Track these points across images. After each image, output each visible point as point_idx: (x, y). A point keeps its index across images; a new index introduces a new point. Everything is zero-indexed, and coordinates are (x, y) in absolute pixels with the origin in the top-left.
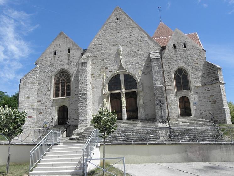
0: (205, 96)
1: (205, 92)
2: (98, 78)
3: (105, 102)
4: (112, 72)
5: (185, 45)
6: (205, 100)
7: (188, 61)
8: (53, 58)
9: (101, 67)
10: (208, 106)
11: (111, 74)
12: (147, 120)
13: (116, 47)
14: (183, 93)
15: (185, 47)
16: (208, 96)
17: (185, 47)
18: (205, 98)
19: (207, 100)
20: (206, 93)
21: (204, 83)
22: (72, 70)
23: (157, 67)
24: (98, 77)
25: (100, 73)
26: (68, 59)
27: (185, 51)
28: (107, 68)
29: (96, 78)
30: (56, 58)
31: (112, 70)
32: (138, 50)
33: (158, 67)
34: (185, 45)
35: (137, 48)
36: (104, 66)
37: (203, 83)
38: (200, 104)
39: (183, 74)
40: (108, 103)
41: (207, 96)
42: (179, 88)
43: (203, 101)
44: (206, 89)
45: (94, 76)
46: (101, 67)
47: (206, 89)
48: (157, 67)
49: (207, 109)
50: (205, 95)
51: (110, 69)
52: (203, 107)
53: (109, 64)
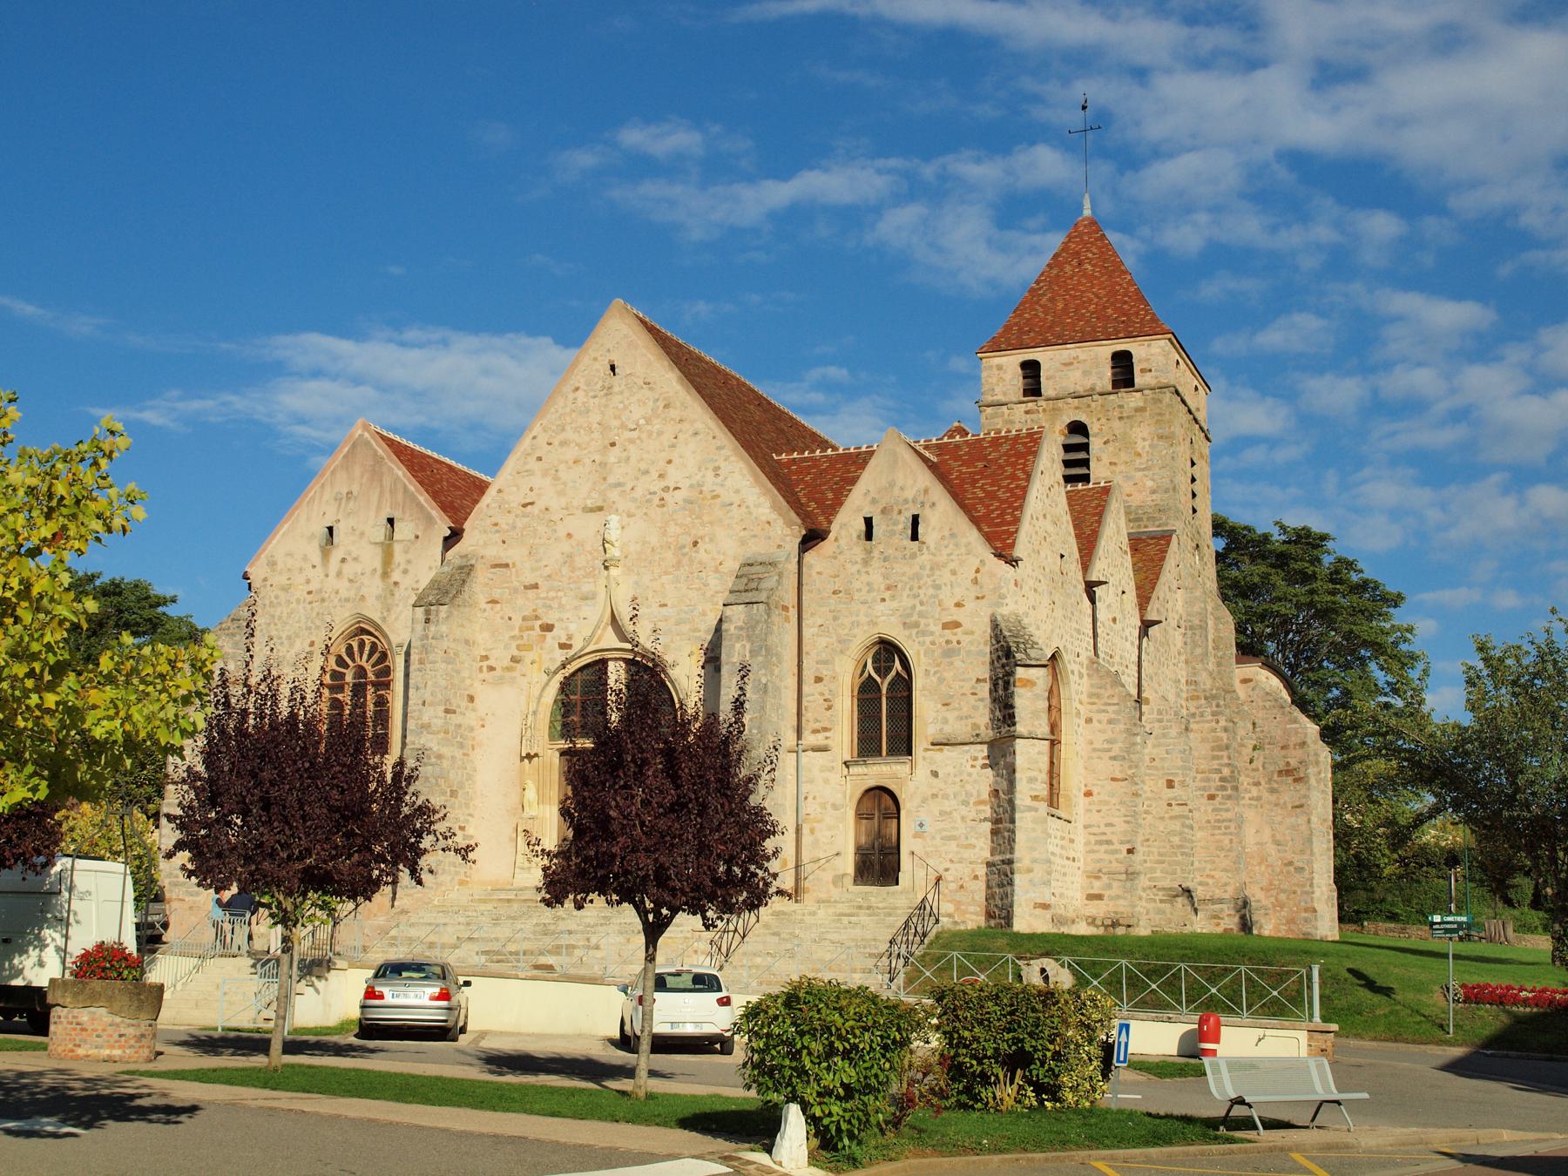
0: (968, 794)
1: (970, 775)
2: (508, 675)
3: (531, 794)
4: (569, 647)
5: (915, 520)
6: (964, 810)
7: (919, 607)
8: (316, 557)
9: (524, 619)
10: (973, 841)
11: (560, 656)
12: (882, 864)
13: (595, 520)
14: (882, 771)
15: (915, 537)
16: (979, 795)
17: (915, 537)
18: (965, 803)
19: (973, 815)
20: (975, 776)
21: (975, 726)
22: (400, 628)
23: (744, 646)
24: (508, 669)
25: (516, 653)
26: (385, 575)
27: (913, 556)
28: (548, 628)
29: (498, 673)
30: (337, 555)
31: (570, 637)
32: (695, 544)
33: (748, 646)
34: (915, 520)
35: (693, 532)
36: (537, 618)
37: (969, 728)
38: (944, 830)
39: (893, 673)
40: (541, 799)
41: (975, 793)
42: (868, 746)
43: (955, 814)
44: (975, 759)
45: (491, 662)
46: (524, 619)
47: (975, 759)
48: (744, 646)
49: (967, 854)
50: (968, 787)
51: (559, 634)
52: (953, 846)
53: (561, 606)
